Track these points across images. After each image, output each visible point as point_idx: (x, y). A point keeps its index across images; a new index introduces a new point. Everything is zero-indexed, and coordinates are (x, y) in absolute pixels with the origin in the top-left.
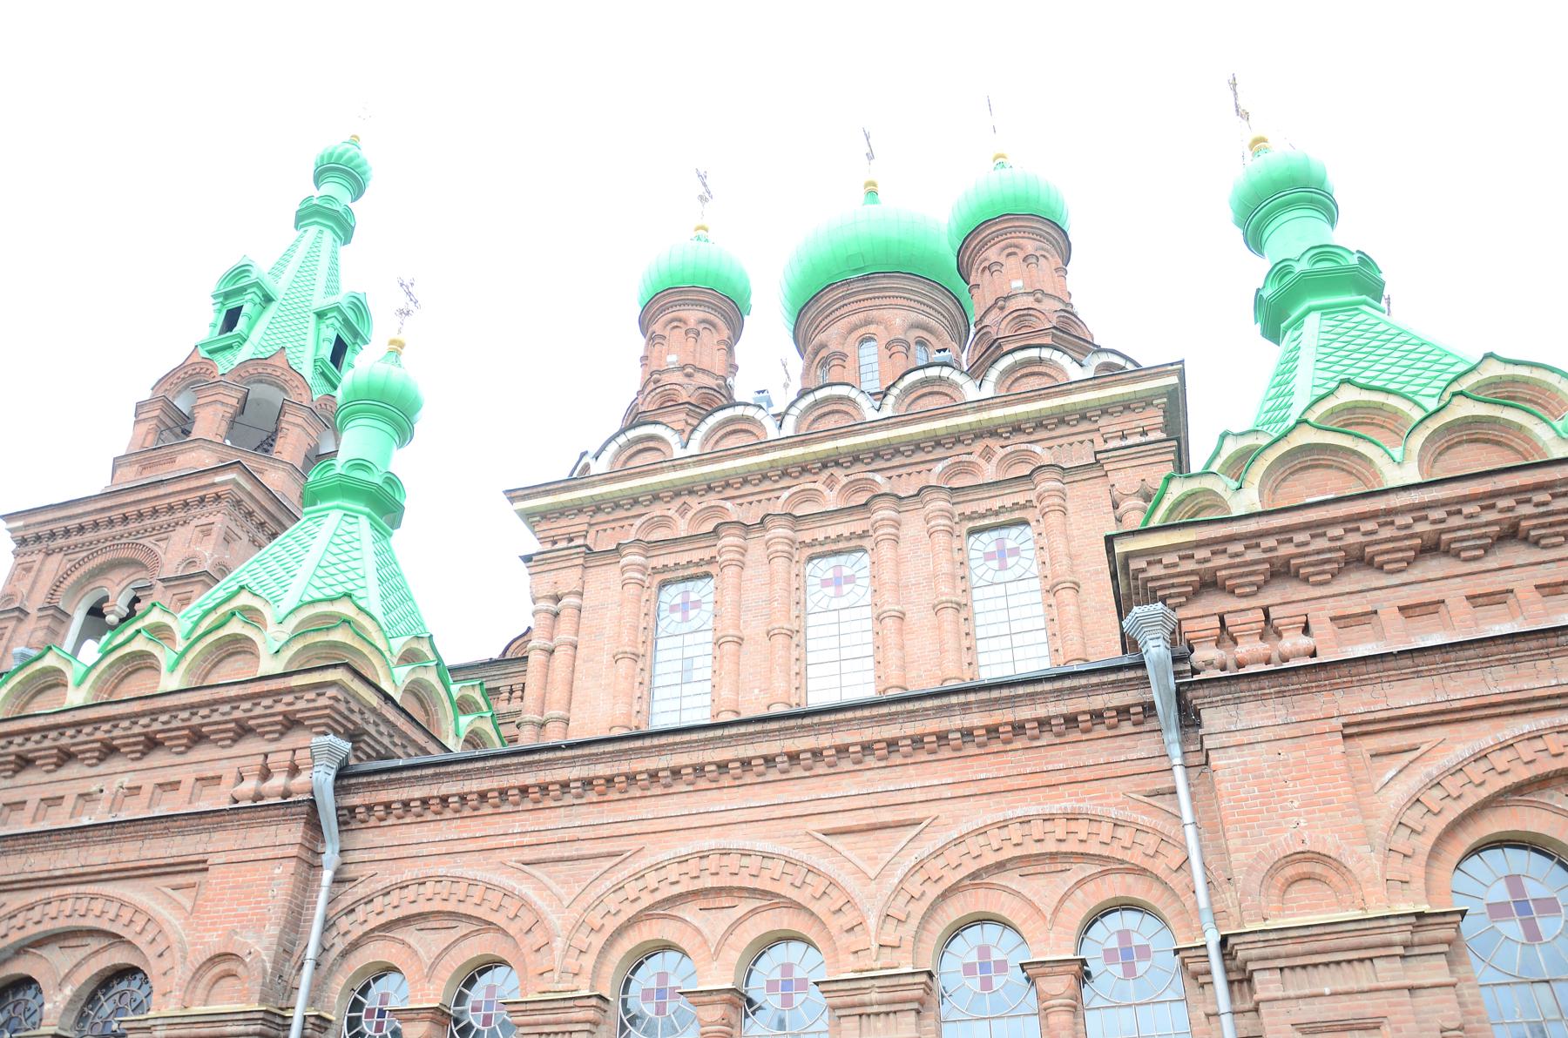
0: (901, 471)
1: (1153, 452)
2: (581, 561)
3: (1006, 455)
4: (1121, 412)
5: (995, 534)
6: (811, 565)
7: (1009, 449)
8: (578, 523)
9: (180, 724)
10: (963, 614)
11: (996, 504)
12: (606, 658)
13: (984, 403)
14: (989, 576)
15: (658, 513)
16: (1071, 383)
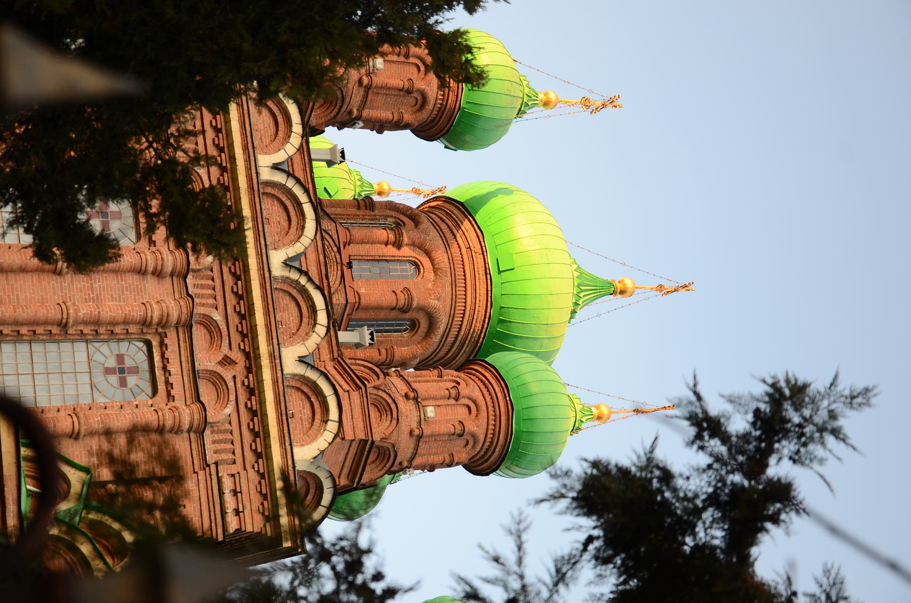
0: (218, 282)
1: (213, 518)
3: (225, 381)
4: (261, 492)
5: (145, 366)
7: (231, 384)
10: (55, 330)
11: (173, 367)
13: (278, 361)
14: (98, 357)
16: (291, 445)
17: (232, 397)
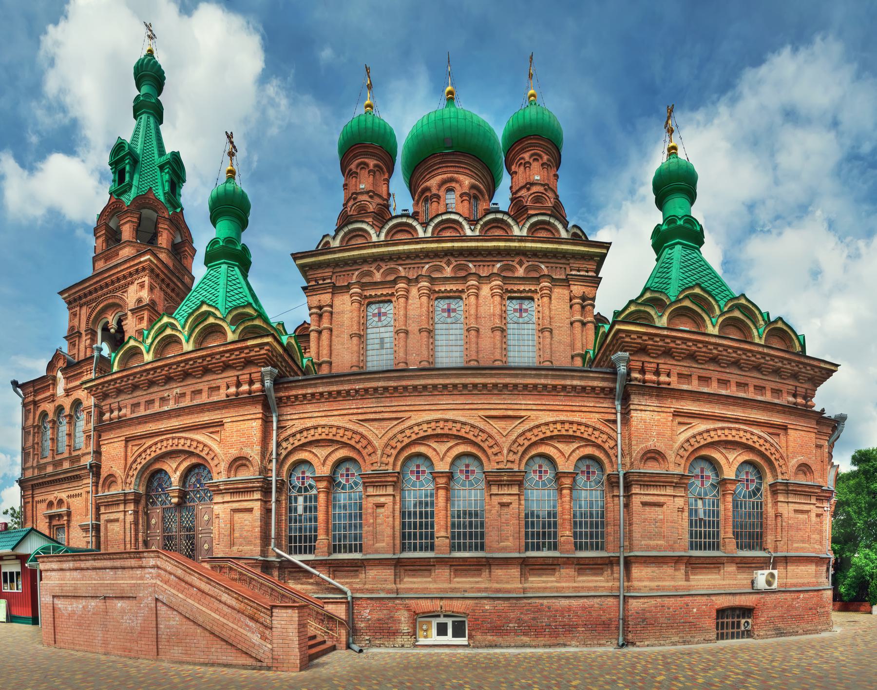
2: (331, 290)
6: (436, 302)
7: (530, 263)
8: (327, 272)
9: (198, 365)
12: (346, 336)
15: (366, 269)
17: (537, 263)
